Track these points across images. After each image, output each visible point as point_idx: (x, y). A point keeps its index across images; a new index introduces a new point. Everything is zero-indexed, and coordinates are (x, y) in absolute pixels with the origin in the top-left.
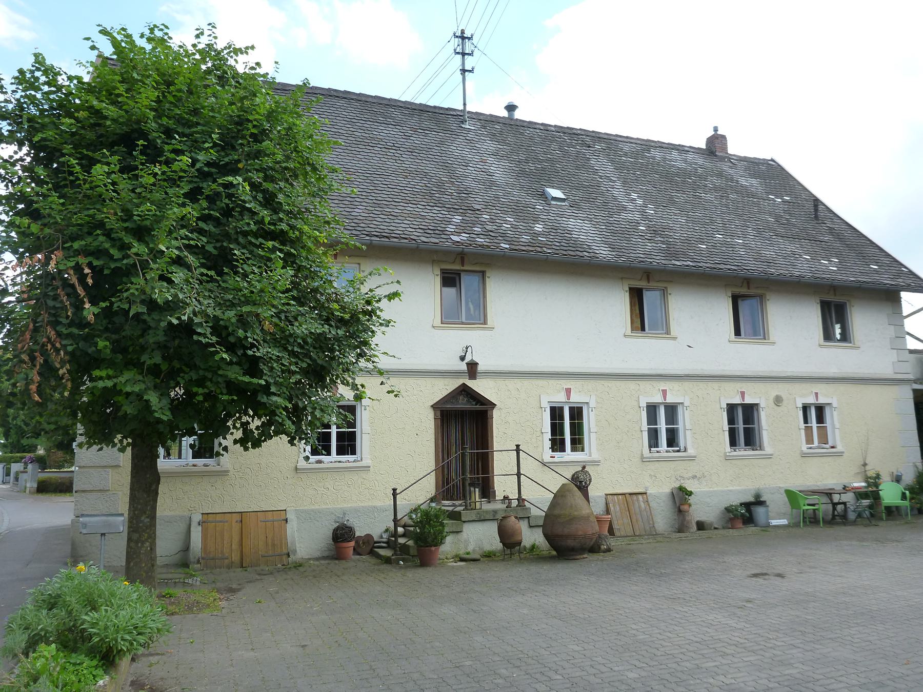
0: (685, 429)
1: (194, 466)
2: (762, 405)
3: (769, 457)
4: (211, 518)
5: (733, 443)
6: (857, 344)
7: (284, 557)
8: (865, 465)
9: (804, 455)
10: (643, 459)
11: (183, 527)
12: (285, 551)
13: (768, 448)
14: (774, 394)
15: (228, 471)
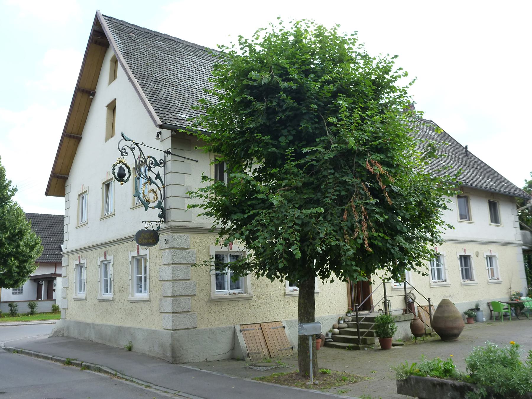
0: (445, 269)
1: (233, 294)
2: (472, 256)
3: (476, 284)
4: (245, 327)
5: (463, 278)
6: (503, 224)
7: (291, 350)
8: (510, 288)
9: (489, 283)
10: (431, 286)
11: (229, 334)
12: (290, 347)
13: (476, 281)
14: (476, 250)
15: (252, 297)
